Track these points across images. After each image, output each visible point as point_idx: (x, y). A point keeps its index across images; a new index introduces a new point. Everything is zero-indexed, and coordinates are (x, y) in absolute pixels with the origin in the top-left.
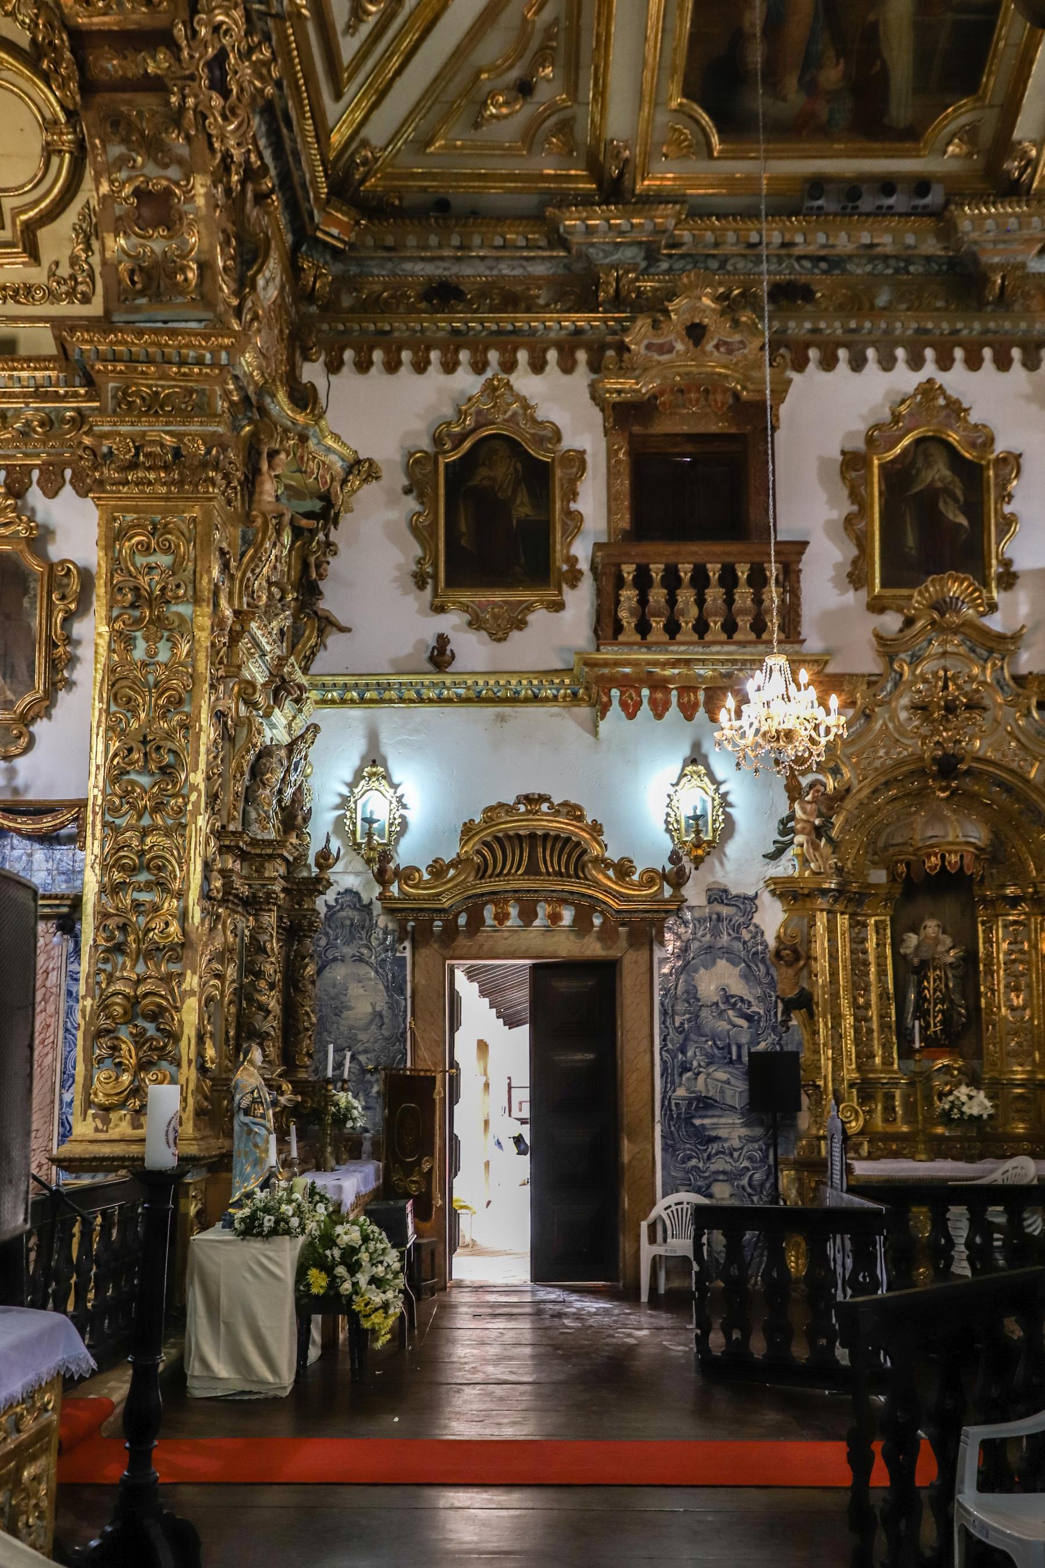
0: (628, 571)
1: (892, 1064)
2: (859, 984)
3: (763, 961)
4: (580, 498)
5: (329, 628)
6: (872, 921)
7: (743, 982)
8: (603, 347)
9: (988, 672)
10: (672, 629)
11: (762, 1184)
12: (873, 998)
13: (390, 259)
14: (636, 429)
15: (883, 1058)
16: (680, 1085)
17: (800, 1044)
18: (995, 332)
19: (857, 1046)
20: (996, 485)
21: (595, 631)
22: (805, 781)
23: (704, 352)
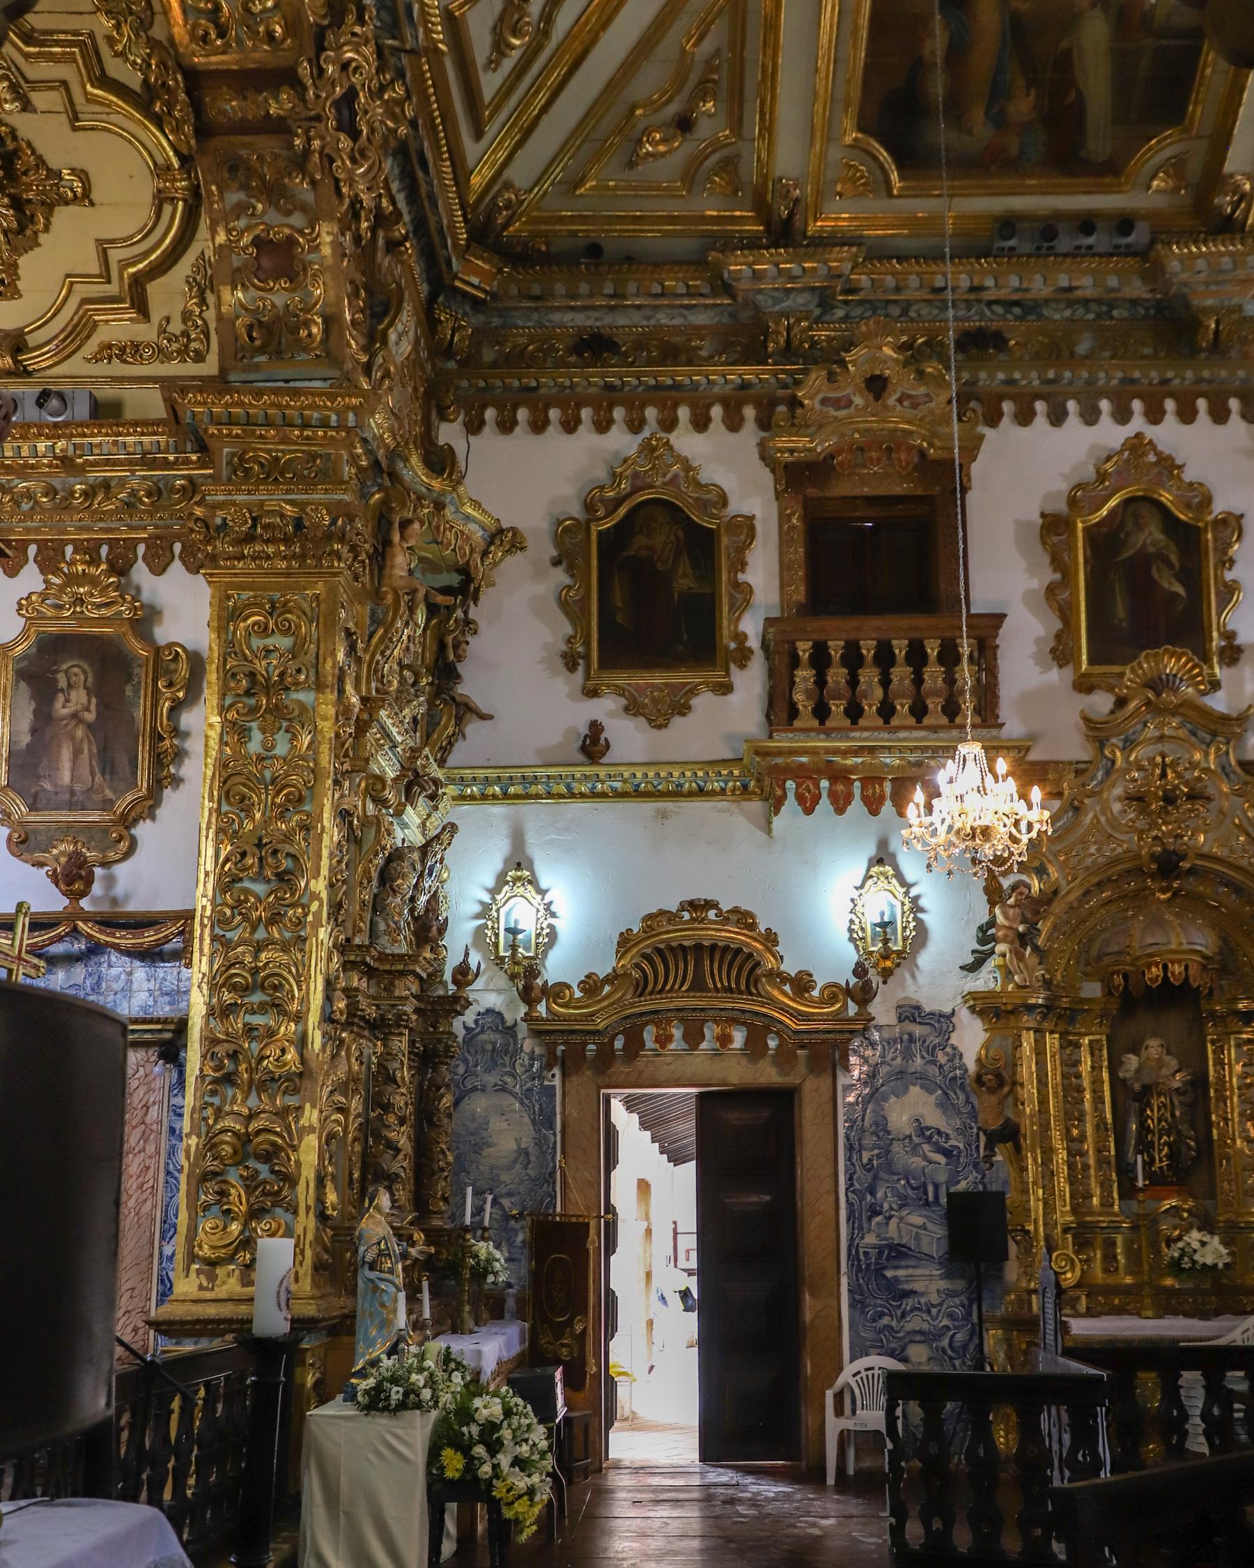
1: (1112, 1205)
2: (1072, 1114)
3: (962, 1087)
6: (1086, 1040)
7: (939, 1111)
8: (773, 402)
9: (1212, 757)
11: (965, 1347)
12: (1089, 1129)
13: (536, 309)
15: (1102, 1197)
16: (869, 1230)
17: (1006, 1182)
19: (1071, 1184)
20: (1215, 549)
22: (1006, 883)
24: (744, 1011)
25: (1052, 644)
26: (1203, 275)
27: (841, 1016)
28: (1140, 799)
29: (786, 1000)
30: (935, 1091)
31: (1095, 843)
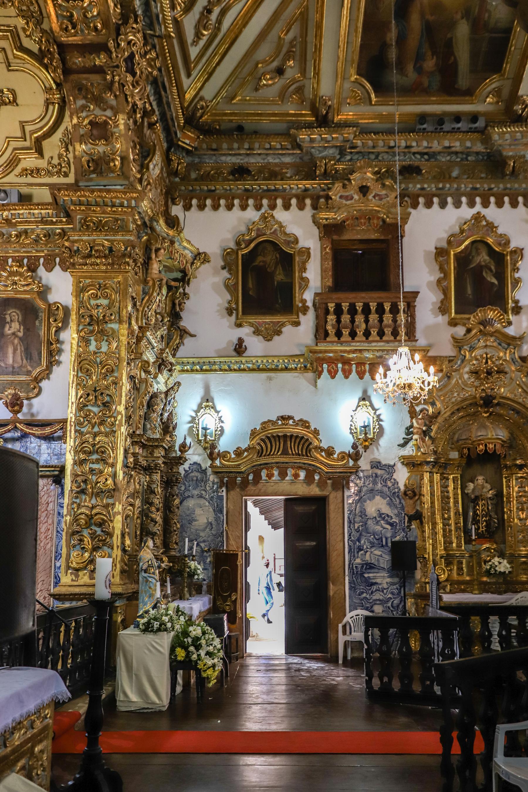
0: (331, 306)
1: (461, 547)
2: (445, 508)
3: (398, 496)
4: (307, 271)
5: (185, 335)
6: (451, 477)
7: (388, 507)
9: (508, 355)
10: (353, 334)
11: (398, 606)
12: (452, 514)
14: (335, 237)
15: (457, 544)
16: (358, 557)
17: (416, 537)
18: (510, 189)
19: (444, 538)
20: (511, 264)
21: (315, 336)
22: (418, 409)
23: (368, 199)
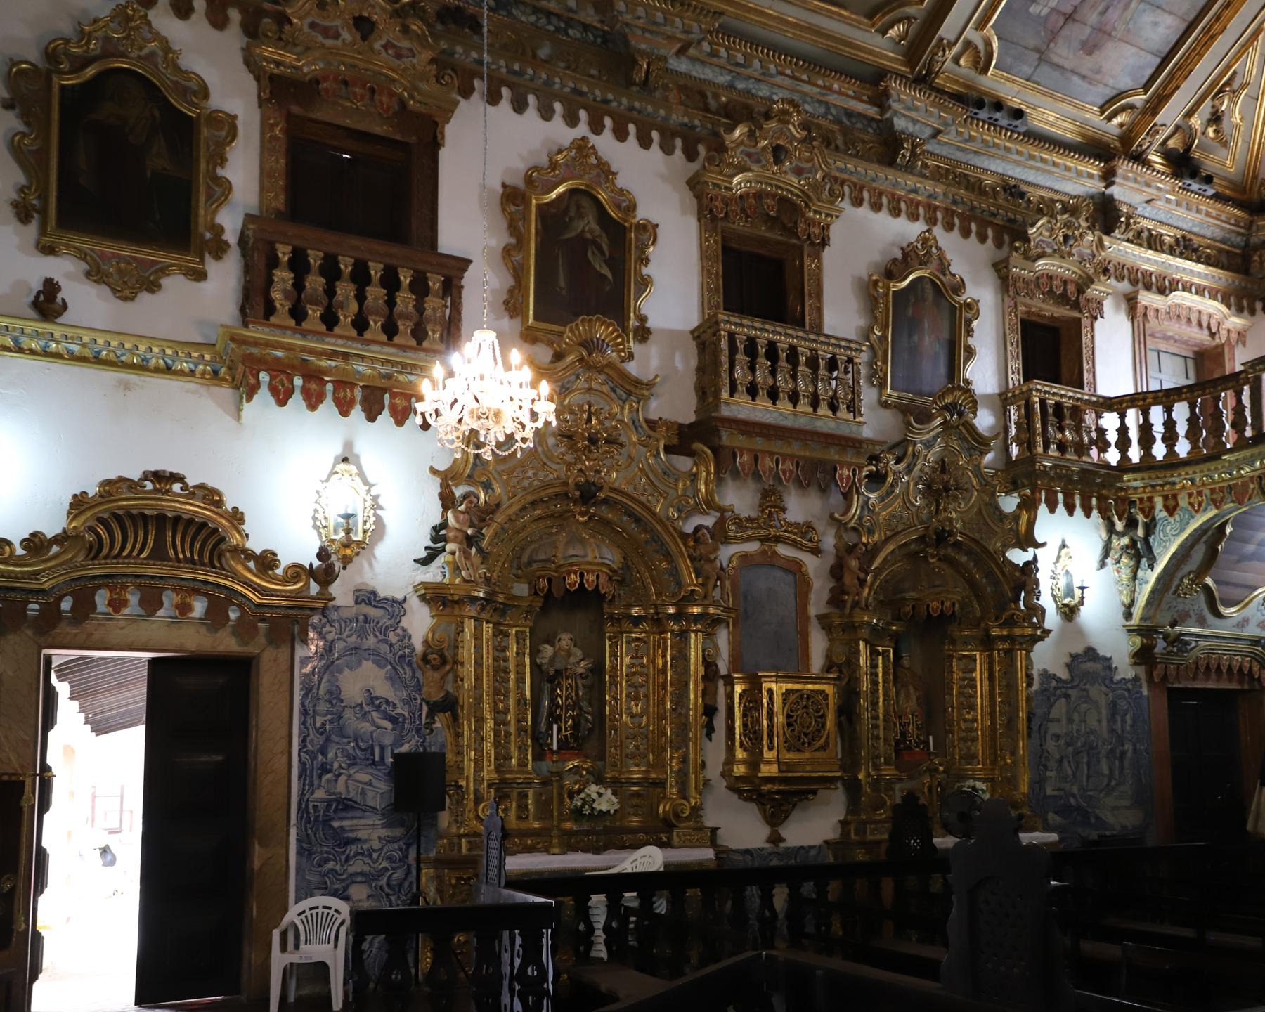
0: (284, 252)
3: (410, 664)
4: (229, 165)
7: (388, 684)
10: (330, 320)
14: (295, 109)
18: (639, 112)
20: (636, 247)
21: (242, 310)
22: (459, 491)
23: (372, 49)
24: (206, 583)
25: (505, 297)
26: (641, 21)
27: (304, 594)
28: (570, 437)
29: (249, 576)
30: (385, 666)
31: (533, 468)
